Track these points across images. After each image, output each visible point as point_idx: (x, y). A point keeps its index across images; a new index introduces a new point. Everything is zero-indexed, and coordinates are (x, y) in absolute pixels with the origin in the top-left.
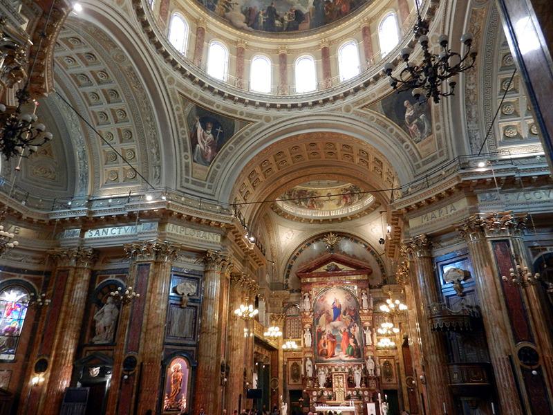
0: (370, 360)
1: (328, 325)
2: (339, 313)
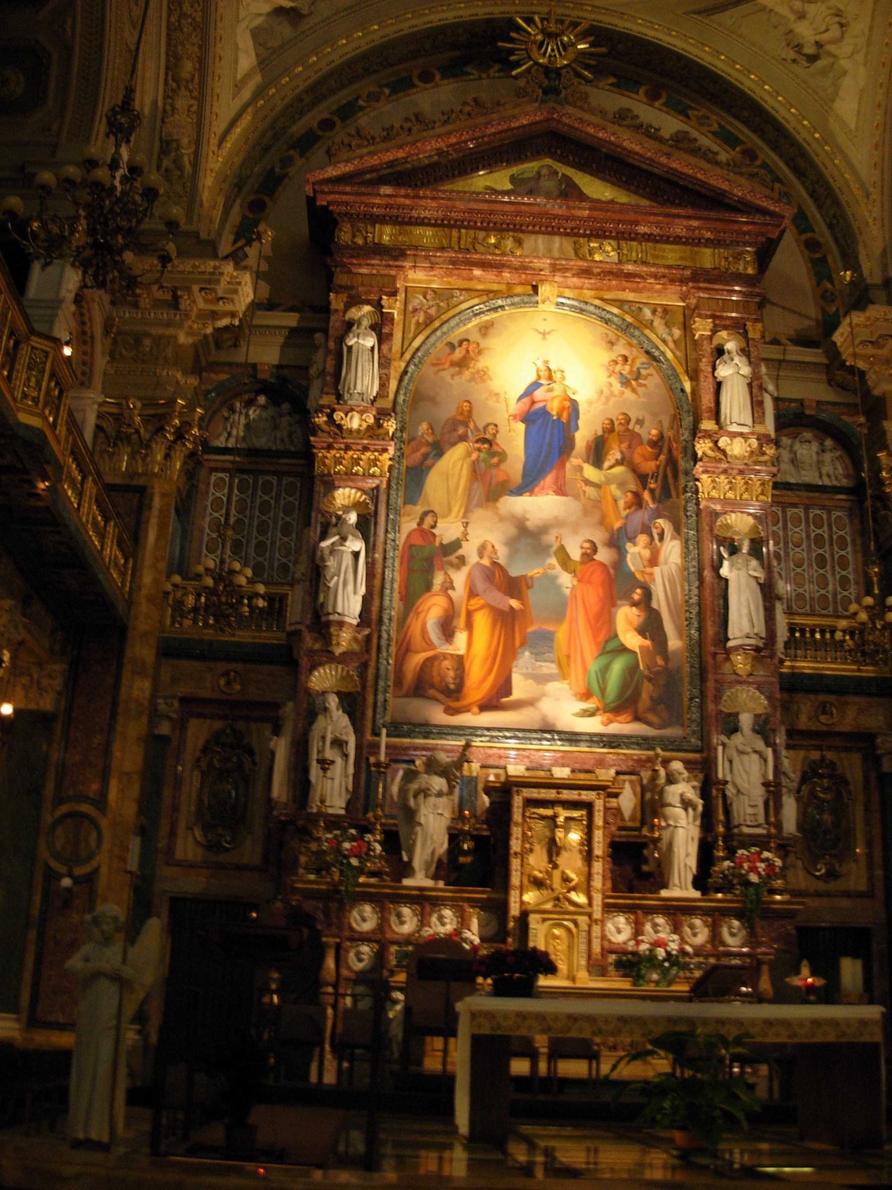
0: (746, 738)
1: (479, 514)
2: (566, 446)
